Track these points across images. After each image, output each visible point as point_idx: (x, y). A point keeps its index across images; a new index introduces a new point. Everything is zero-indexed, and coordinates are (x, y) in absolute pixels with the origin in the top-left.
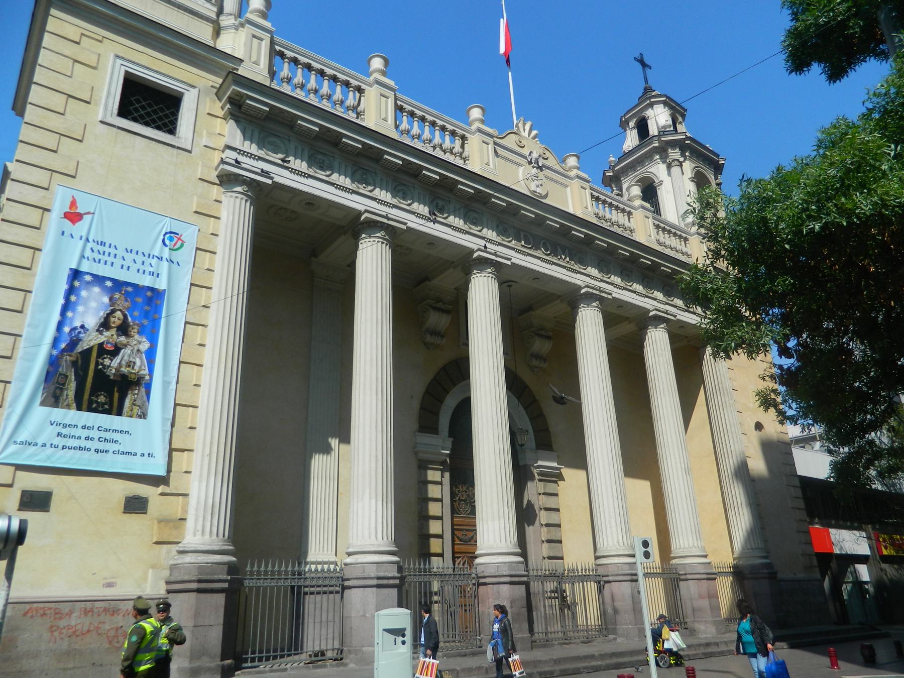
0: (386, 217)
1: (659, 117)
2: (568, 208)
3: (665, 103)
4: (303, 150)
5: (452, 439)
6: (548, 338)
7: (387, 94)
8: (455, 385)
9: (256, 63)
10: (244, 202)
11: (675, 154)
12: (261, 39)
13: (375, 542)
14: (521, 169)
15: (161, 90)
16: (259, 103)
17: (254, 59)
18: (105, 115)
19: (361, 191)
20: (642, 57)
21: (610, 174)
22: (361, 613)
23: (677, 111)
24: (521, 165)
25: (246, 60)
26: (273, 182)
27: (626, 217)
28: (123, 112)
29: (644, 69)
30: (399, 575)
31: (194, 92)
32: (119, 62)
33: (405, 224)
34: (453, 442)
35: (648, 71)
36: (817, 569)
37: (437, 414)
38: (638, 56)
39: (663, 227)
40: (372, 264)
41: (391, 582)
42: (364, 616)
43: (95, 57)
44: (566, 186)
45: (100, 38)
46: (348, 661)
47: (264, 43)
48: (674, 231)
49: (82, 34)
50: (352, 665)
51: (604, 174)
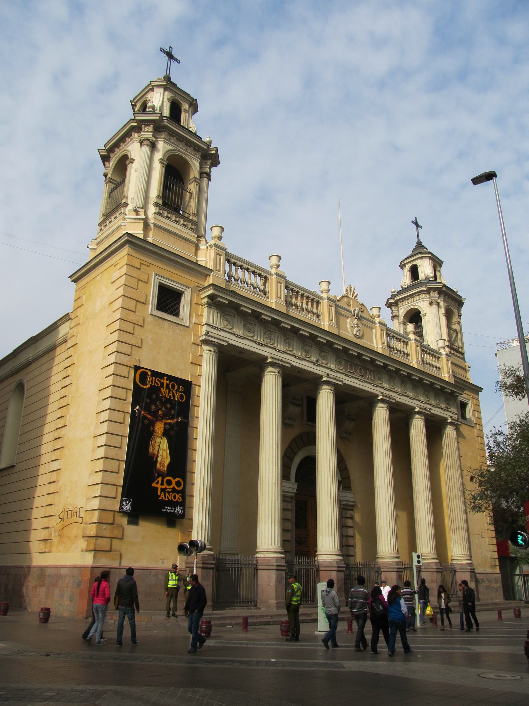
0: (281, 361)
1: (425, 269)
2: (372, 342)
3: (430, 258)
4: (241, 322)
5: (297, 483)
6: (353, 420)
7: (281, 281)
8: (300, 450)
9: (219, 271)
10: (212, 356)
11: (435, 296)
12: (221, 255)
13: (270, 547)
14: (349, 320)
15: (173, 290)
16: (225, 298)
17: (218, 269)
18: (152, 311)
19: (269, 345)
20: (416, 220)
21: (392, 301)
22: (268, 583)
23: (437, 263)
24: (348, 317)
25: (215, 270)
26: (228, 344)
27: (405, 346)
29: (417, 229)
30: (285, 564)
31: (189, 290)
32: (157, 277)
33: (290, 364)
34: (298, 485)
35: (420, 229)
36: (498, 567)
37: (290, 468)
38: (414, 220)
39: (426, 350)
40: (271, 387)
41: (283, 568)
42: (269, 585)
43: (146, 276)
44: (372, 329)
45: (148, 264)
46: (261, 607)
47: (222, 257)
48: (432, 353)
49: (141, 263)
50: (263, 609)
51: (388, 300)
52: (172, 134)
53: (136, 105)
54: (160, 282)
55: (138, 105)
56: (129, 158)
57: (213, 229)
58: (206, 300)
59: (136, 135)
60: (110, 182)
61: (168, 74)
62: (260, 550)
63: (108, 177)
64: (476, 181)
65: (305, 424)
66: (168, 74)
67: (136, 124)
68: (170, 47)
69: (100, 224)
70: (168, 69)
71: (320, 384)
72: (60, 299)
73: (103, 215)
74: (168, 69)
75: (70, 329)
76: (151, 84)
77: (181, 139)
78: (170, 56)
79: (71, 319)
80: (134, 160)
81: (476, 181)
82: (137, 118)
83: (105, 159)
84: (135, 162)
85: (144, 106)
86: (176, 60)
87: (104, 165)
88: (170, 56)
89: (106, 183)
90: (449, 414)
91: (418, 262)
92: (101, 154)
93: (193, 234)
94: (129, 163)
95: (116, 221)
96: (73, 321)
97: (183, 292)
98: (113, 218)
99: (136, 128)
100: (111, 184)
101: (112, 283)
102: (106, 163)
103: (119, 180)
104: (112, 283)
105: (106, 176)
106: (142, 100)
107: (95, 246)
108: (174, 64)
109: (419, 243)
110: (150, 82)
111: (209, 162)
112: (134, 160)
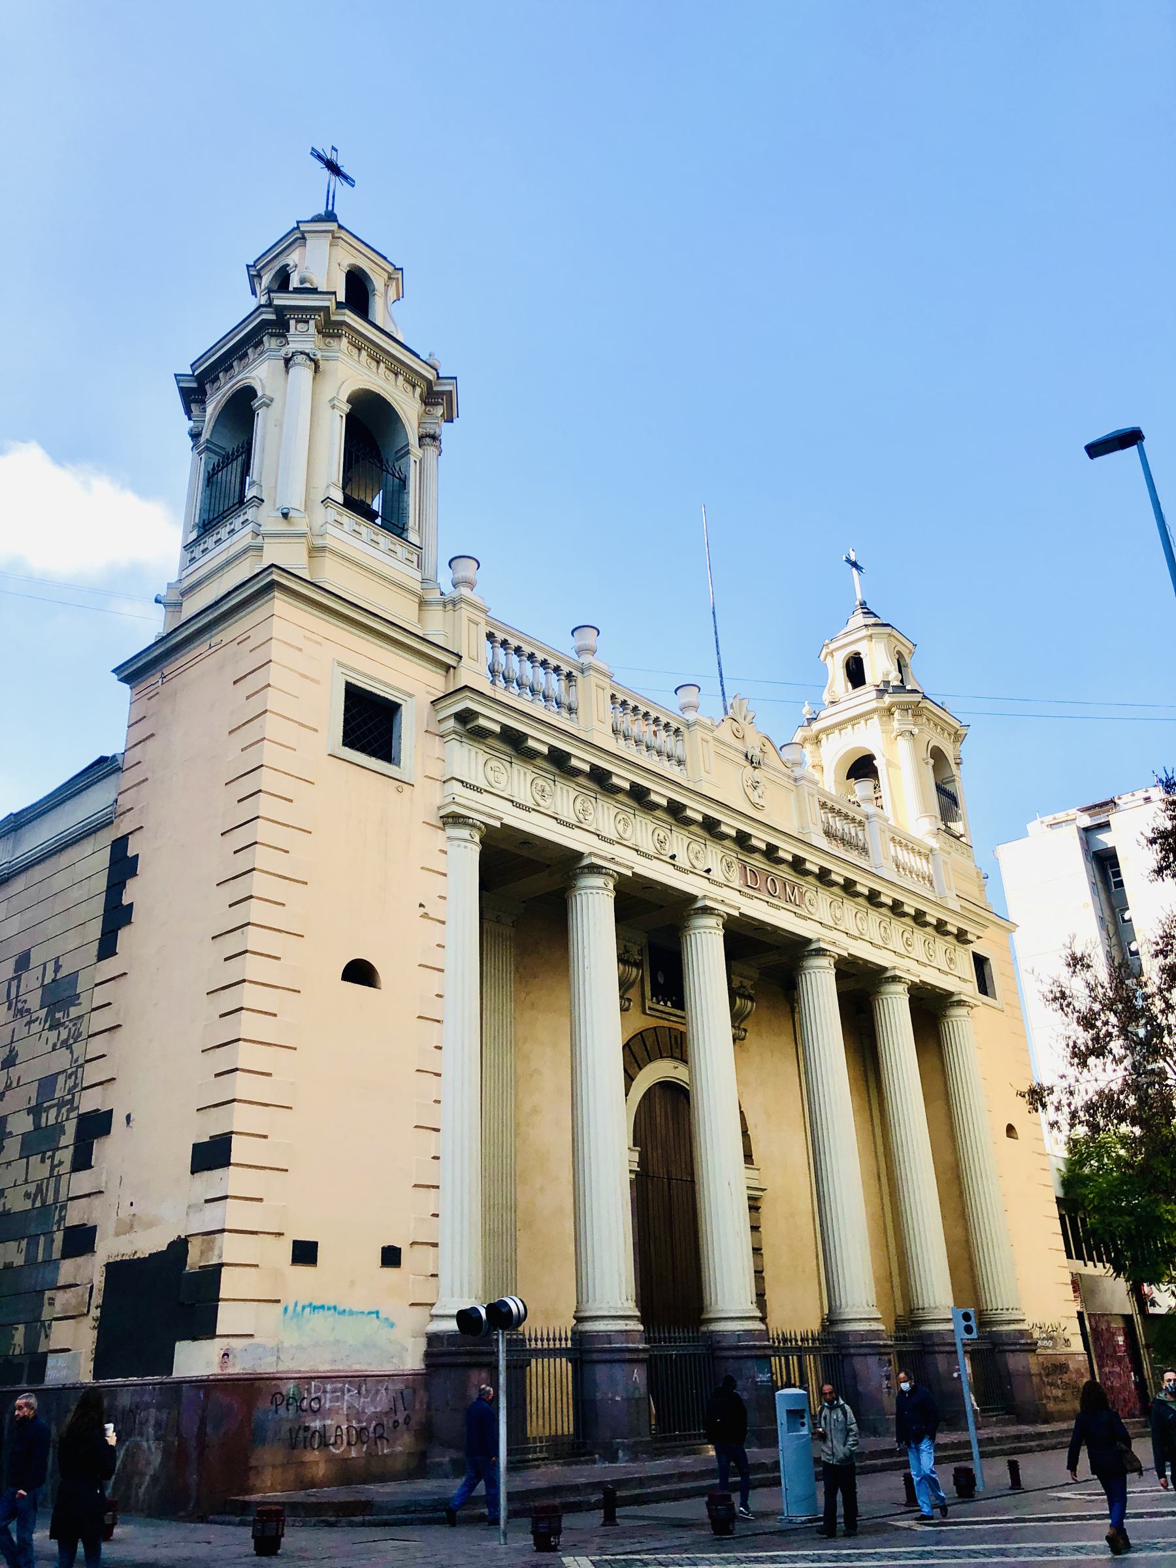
28: (352, 739)
52: (361, 343)
53: (259, 276)
54: (348, 684)
55: (266, 279)
56: (260, 394)
57: (453, 564)
58: (451, 723)
59: (270, 343)
60: (207, 449)
61: (330, 208)
62: (587, 1314)
63: (202, 439)
64: (1096, 450)
65: (650, 1008)
66: (330, 208)
67: (273, 317)
68: (333, 148)
69: (187, 547)
71: (690, 915)
72: (103, 721)
74: (330, 197)
76: (298, 227)
77: (379, 356)
78: (333, 167)
79: (120, 769)
81: (1096, 450)
82: (276, 302)
83: (192, 395)
84: (274, 404)
85: (282, 281)
86: (346, 177)
87: (188, 412)
88: (333, 167)
89: (200, 454)
92: (182, 385)
94: (260, 406)
95: (235, 536)
97: (400, 705)
98: (223, 532)
99: (277, 324)
100: (212, 455)
101: (235, 683)
102: (193, 406)
103: (230, 445)
105: (195, 436)
106: (277, 265)
107: (174, 597)
110: (298, 222)
111: (439, 411)
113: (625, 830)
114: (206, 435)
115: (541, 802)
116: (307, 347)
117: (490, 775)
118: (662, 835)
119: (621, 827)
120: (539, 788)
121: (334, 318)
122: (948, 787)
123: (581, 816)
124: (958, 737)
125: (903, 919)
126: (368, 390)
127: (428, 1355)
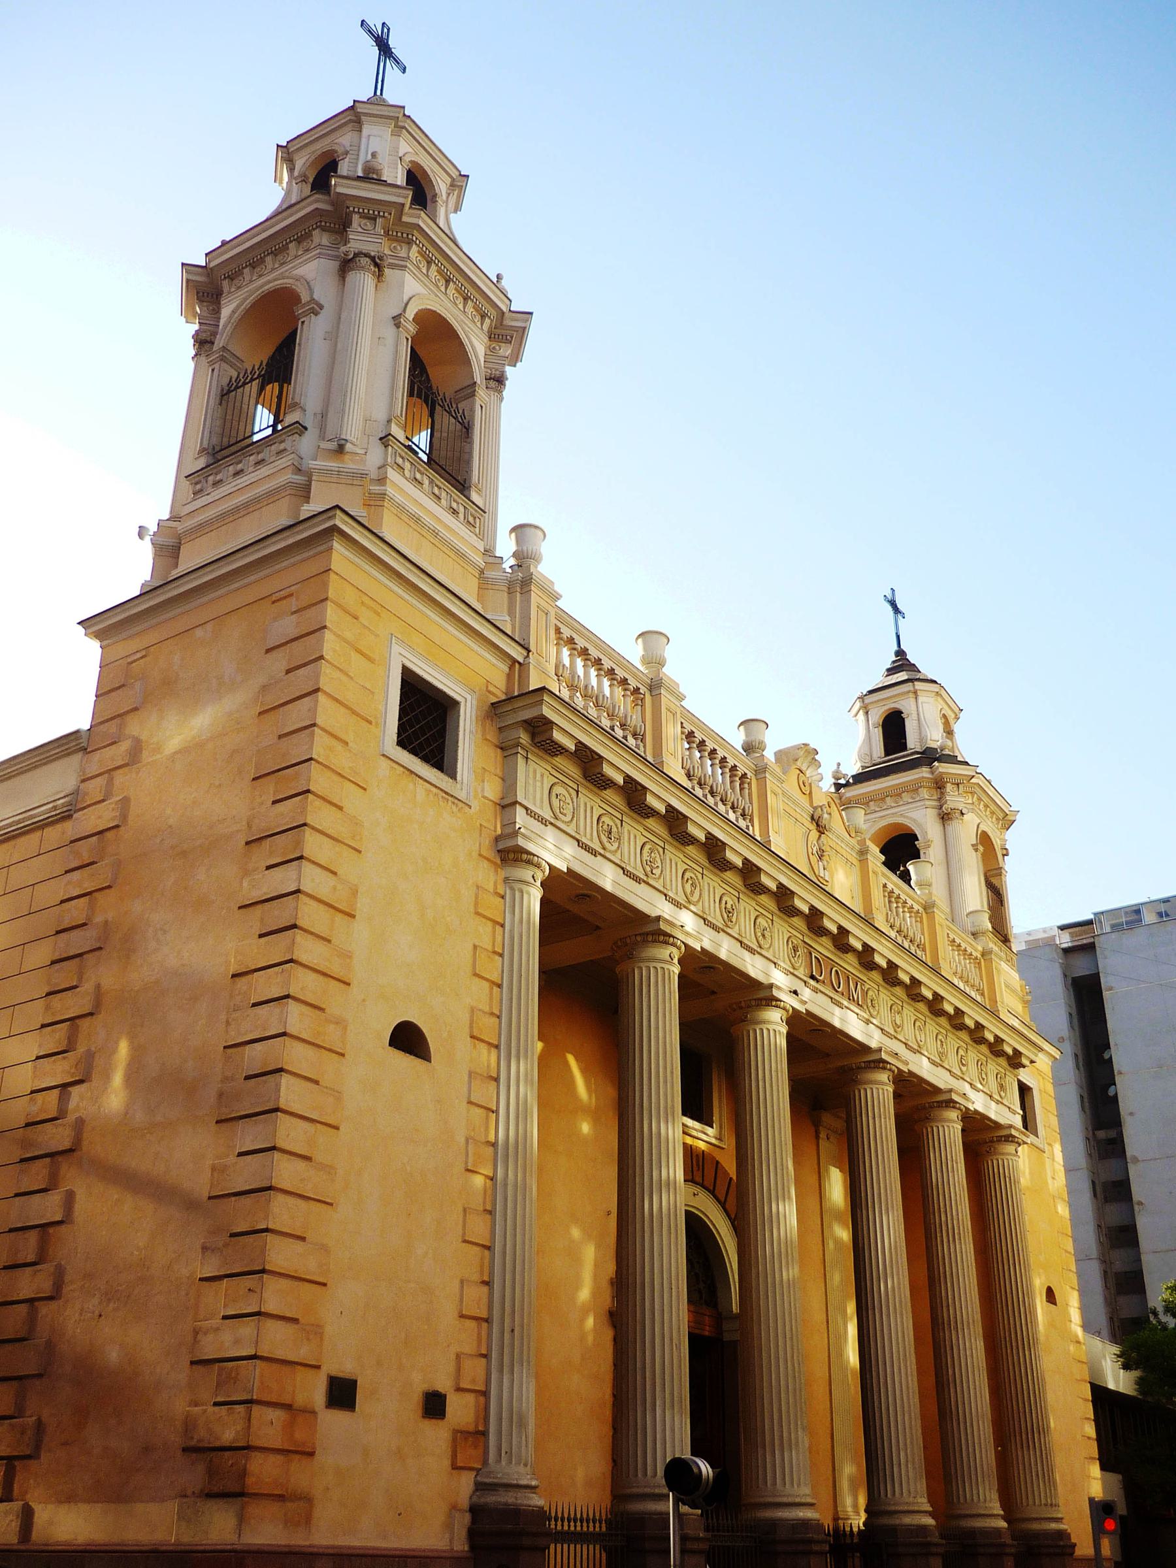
56: (305, 298)
60: (223, 359)
70: (380, 81)
73: (203, 450)
74: (380, 81)
75: (83, 781)
80: (321, 307)
89: (211, 363)
90: (1006, 1114)
91: (907, 706)
93: (474, 540)
94: (306, 314)
96: (97, 756)
100: (225, 366)
101: (268, 651)
104: (268, 651)
108: (392, 71)
109: (900, 653)
112: (321, 307)
113: (692, 893)
114: (219, 342)
115: (607, 845)
116: (373, 249)
117: (555, 802)
118: (730, 903)
119: (688, 887)
120: (605, 827)
121: (405, 219)
122: (994, 881)
123: (648, 869)
124: (1007, 821)
125: (960, 1033)
126: (430, 310)
127: (472, 1534)
